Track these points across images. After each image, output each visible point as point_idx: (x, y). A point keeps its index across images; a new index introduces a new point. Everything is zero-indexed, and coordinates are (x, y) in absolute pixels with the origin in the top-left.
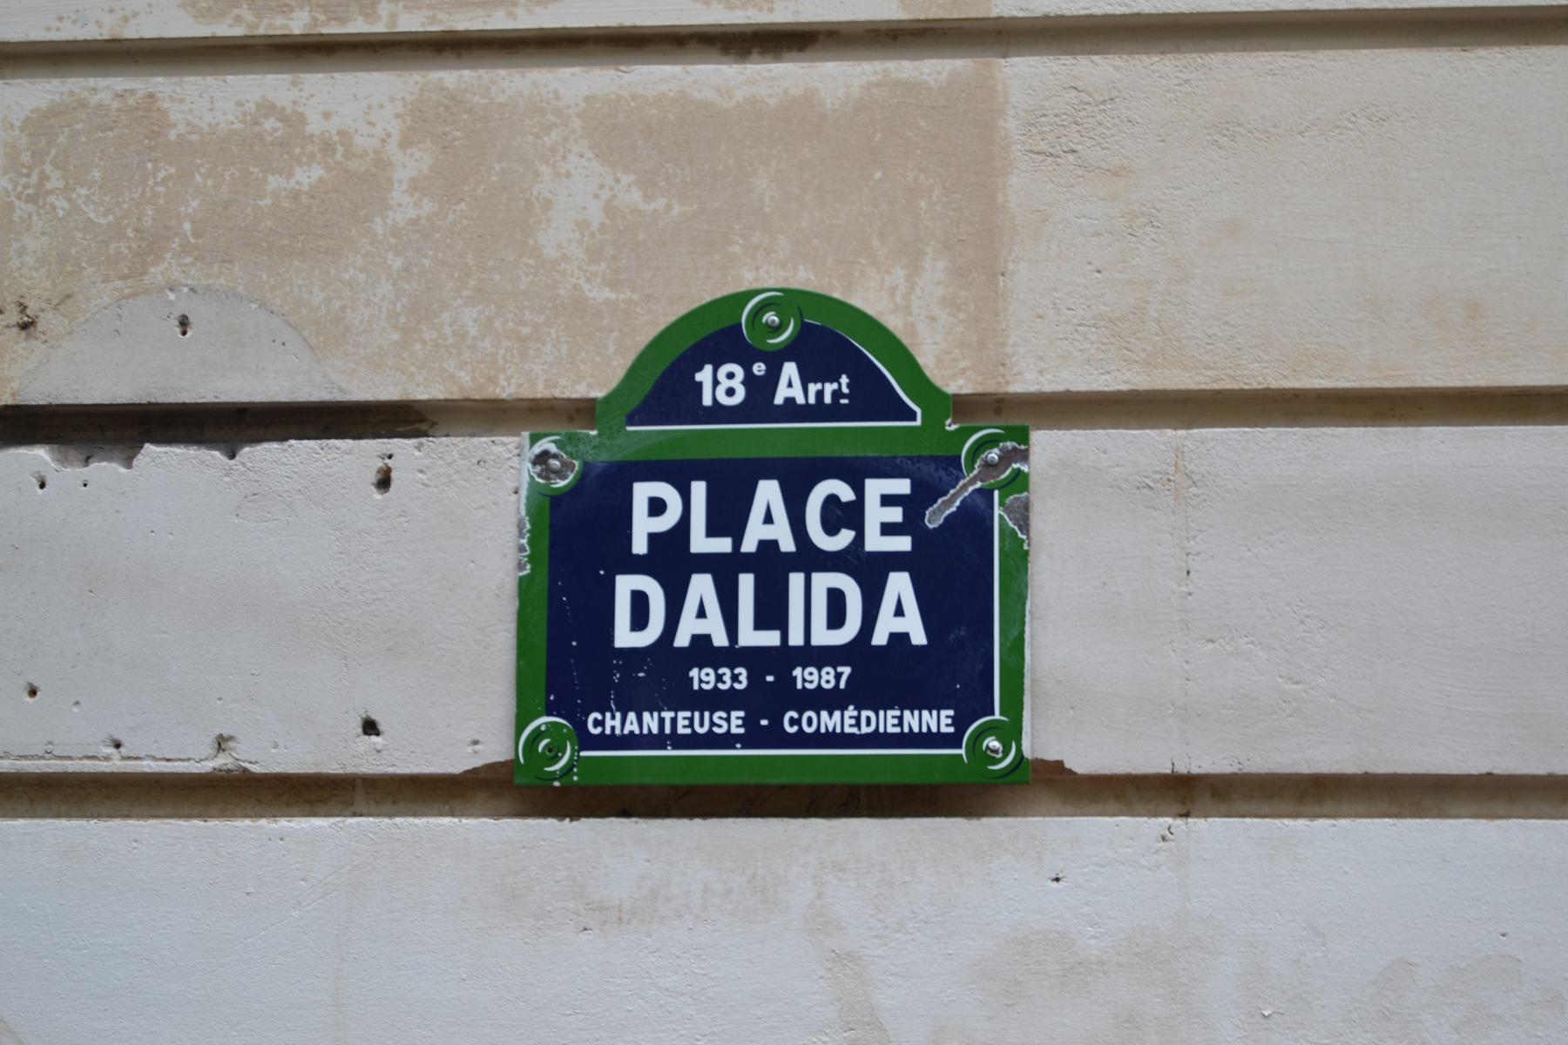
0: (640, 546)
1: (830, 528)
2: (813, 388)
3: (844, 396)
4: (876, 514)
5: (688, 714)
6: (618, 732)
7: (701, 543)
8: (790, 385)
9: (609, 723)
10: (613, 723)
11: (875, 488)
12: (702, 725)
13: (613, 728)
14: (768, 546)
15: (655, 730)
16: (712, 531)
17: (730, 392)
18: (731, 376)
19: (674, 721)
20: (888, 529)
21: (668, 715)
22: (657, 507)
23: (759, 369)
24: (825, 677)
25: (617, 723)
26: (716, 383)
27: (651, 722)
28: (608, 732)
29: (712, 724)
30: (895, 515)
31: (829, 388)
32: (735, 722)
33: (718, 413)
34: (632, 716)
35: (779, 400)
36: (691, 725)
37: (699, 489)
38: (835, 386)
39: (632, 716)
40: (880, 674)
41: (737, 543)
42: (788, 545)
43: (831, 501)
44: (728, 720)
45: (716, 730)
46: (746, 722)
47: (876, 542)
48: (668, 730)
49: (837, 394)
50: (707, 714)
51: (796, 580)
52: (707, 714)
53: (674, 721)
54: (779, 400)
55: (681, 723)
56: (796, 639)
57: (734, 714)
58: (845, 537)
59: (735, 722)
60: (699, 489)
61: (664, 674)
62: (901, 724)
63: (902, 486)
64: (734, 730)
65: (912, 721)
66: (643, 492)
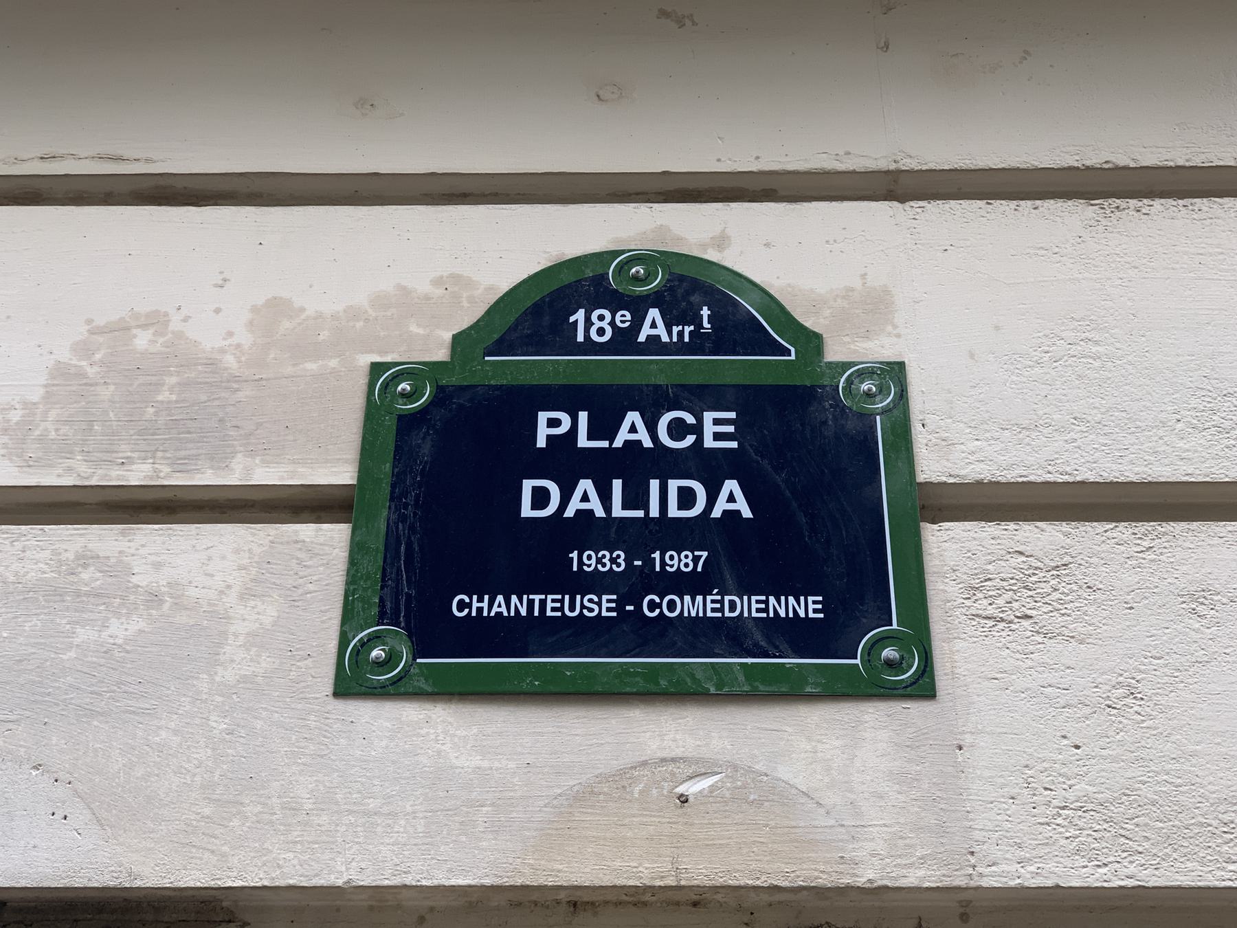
2: (675, 329)
12: (572, 609)
19: (543, 603)
21: (537, 598)
25: (485, 605)
26: (588, 323)
29: (583, 606)
33: (590, 347)
34: (500, 598)
35: (642, 338)
36: (561, 609)
39: (500, 598)
44: (599, 604)
48: (536, 613)
52: (578, 597)
53: (543, 603)
54: (642, 338)
55: (550, 605)
57: (605, 597)
62: (766, 610)
64: (604, 613)
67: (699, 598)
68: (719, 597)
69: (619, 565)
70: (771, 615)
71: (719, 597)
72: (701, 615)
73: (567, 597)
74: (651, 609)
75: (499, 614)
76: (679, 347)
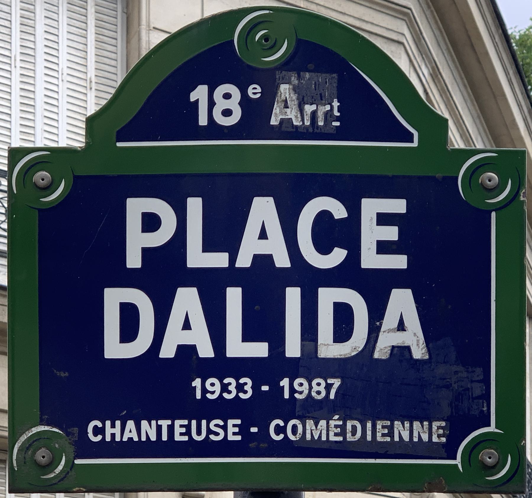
0: (134, 260)
4: (371, 233)
5: (186, 422)
6: (118, 439)
7: (197, 257)
9: (109, 431)
12: (199, 433)
13: (113, 435)
14: (263, 261)
15: (153, 438)
19: (171, 428)
20: (383, 247)
21: (165, 423)
22: (151, 223)
25: (117, 430)
27: (149, 430)
28: (108, 439)
29: (209, 431)
32: (232, 430)
34: (131, 424)
36: (188, 433)
39: (131, 424)
41: (233, 259)
42: (282, 260)
44: (225, 428)
45: (212, 437)
46: (243, 430)
47: (371, 259)
48: (165, 438)
50: (204, 422)
51: (293, 296)
53: (171, 428)
55: (178, 430)
57: (231, 422)
58: (338, 256)
59: (231, 430)
60: (195, 206)
63: (398, 206)
64: (231, 438)
67: (323, 423)
69: (246, 392)
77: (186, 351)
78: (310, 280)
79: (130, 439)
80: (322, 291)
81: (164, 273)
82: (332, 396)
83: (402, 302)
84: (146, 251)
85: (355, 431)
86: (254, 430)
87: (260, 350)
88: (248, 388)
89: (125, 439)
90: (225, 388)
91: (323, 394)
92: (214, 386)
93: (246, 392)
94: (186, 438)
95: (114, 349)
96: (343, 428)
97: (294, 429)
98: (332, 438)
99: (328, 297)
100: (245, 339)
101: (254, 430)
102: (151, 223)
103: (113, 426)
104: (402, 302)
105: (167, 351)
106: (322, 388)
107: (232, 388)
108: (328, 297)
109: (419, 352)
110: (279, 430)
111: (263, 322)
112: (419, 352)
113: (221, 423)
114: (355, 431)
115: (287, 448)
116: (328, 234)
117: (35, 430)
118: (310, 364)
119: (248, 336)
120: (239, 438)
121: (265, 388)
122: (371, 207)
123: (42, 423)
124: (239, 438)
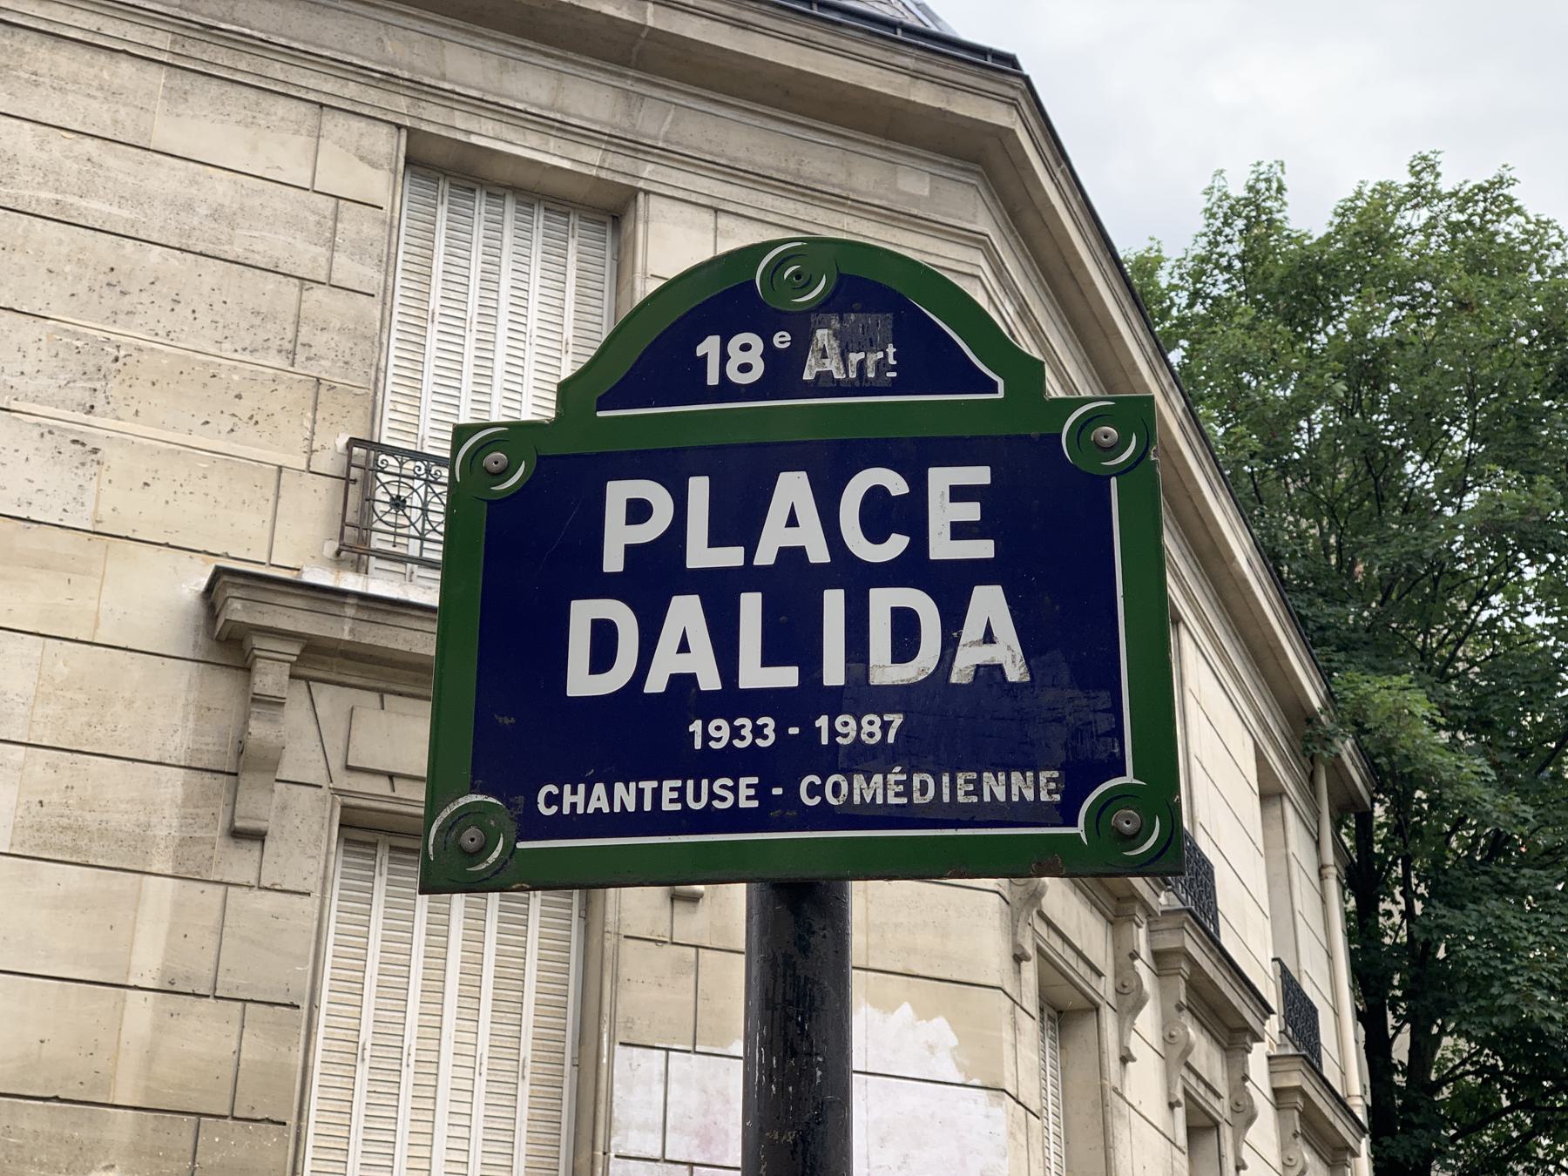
0: (613, 561)
1: (875, 531)
2: (855, 358)
3: (893, 368)
4: (942, 513)
5: (678, 783)
6: (580, 810)
7: (700, 554)
8: (825, 357)
9: (568, 799)
10: (573, 799)
11: (940, 479)
12: (697, 798)
13: (574, 806)
14: (792, 556)
15: (631, 808)
16: (716, 540)
17: (745, 368)
18: (746, 348)
19: (657, 794)
20: (960, 531)
21: (648, 786)
23: (781, 340)
24: (866, 728)
25: (580, 799)
26: (724, 357)
27: (625, 796)
28: (566, 810)
29: (713, 796)
30: (971, 512)
31: (874, 357)
33: (726, 390)
34: (599, 789)
35: (808, 376)
36: (682, 798)
37: (699, 489)
38: (880, 355)
39: (599, 789)
40: (952, 723)
41: (750, 555)
42: (819, 553)
43: (876, 495)
44: (735, 790)
45: (717, 804)
46: (761, 792)
47: (942, 547)
48: (647, 807)
49: (881, 365)
50: (705, 782)
51: (834, 602)
52: (705, 782)
53: (657, 794)
55: (667, 795)
56: (834, 672)
57: (743, 781)
58: (897, 545)
59: (744, 792)
60: (699, 489)
61: (647, 731)
62: (978, 791)
63: (980, 475)
64: (743, 804)
65: (994, 786)
66: (619, 493)
67: (878, 778)
68: (904, 777)
69: (765, 737)
70: (987, 798)
71: (904, 777)
72: (879, 801)
73: (690, 783)
74: (811, 795)
75: (598, 810)
76: (860, 386)
77: (683, 683)
78: (858, 579)
79: (598, 810)
80: (874, 593)
81: (654, 577)
82: (891, 739)
83: (988, 603)
84: (630, 550)
85: (926, 788)
86: (777, 791)
87: (787, 677)
88: (770, 731)
89: (590, 810)
90: (736, 733)
91: (878, 736)
92: (720, 730)
93: (765, 737)
94: (678, 807)
95: (581, 682)
96: (908, 784)
97: (836, 788)
98: (892, 800)
99: (883, 601)
100: (766, 662)
101: (777, 791)
102: (638, 511)
103: (574, 792)
104: (988, 603)
105: (656, 683)
106: (876, 729)
107: (746, 732)
108: (883, 601)
109: (1016, 672)
110: (814, 790)
111: (792, 638)
112: (1016, 672)
113: (730, 783)
114: (926, 788)
115: (825, 817)
116: (881, 515)
117: (462, 801)
118: (860, 695)
119: (770, 658)
120: (755, 804)
121: (794, 731)
122: (940, 479)
123: (473, 790)
124: (755, 804)
